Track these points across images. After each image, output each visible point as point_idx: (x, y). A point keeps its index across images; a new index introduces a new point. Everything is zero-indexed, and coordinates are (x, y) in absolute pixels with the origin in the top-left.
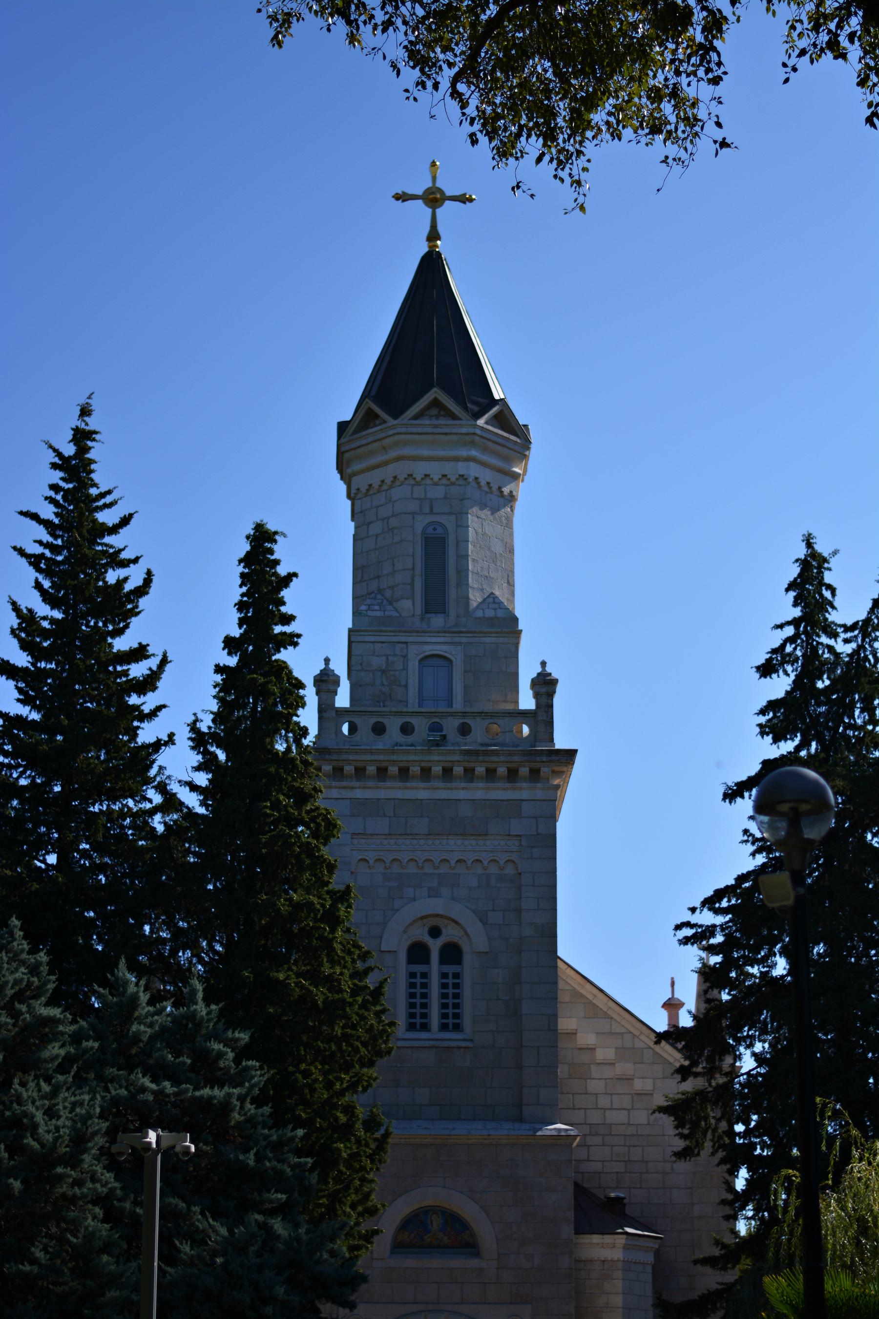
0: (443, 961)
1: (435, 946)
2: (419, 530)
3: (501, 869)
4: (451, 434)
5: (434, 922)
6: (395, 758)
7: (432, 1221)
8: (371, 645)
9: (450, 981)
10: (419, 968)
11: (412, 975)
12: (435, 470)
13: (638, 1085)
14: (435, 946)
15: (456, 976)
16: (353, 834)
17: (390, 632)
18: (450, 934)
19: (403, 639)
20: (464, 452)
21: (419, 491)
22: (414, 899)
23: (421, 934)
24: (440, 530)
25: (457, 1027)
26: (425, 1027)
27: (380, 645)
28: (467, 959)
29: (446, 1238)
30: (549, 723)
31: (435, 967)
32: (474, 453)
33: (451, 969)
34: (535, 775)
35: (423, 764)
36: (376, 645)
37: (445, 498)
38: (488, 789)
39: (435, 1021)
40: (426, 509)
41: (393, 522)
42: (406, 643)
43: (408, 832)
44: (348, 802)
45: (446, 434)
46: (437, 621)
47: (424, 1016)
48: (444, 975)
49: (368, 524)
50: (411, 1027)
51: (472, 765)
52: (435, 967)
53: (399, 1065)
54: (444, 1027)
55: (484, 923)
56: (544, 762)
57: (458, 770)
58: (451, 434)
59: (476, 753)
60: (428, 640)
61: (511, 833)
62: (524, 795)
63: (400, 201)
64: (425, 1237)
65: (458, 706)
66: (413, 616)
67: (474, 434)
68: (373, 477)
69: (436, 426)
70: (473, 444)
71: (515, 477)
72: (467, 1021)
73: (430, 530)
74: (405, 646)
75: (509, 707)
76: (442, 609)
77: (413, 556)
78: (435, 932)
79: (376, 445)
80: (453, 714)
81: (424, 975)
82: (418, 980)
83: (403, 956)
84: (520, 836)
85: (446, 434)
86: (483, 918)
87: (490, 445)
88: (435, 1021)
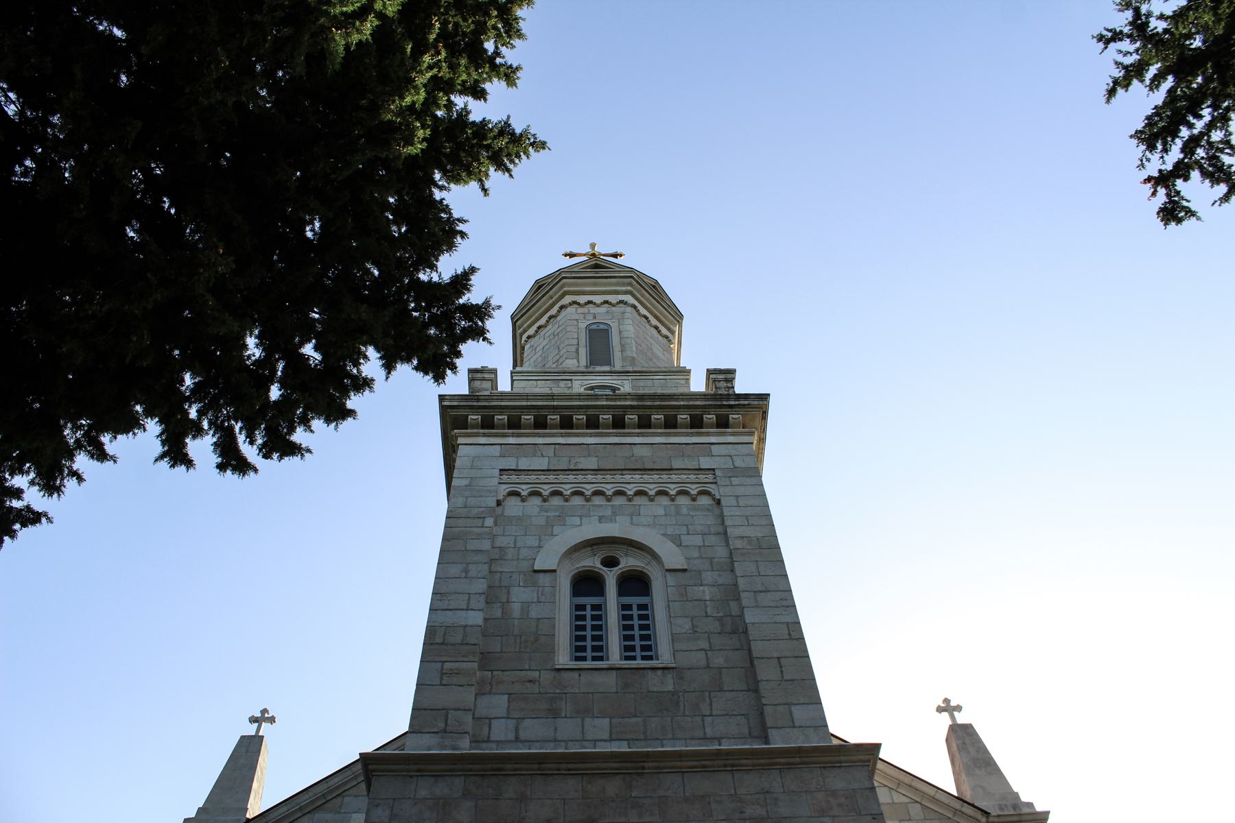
0: (621, 593)
2: (583, 325)
3: (694, 500)
4: (610, 277)
6: (555, 403)
8: (535, 382)
10: (589, 601)
12: (598, 299)
16: (501, 470)
17: (554, 373)
18: (629, 562)
19: (568, 378)
20: (624, 288)
21: (581, 310)
22: (581, 525)
23: (593, 562)
24: (602, 327)
27: (544, 382)
32: (629, 288)
34: (723, 423)
35: (590, 412)
36: (539, 382)
37: (607, 312)
38: (668, 435)
40: (590, 317)
41: (557, 331)
42: (571, 380)
43: (572, 467)
44: (499, 446)
45: (606, 277)
49: (536, 349)
51: (648, 412)
53: (558, 691)
55: (680, 545)
56: (731, 406)
57: (632, 417)
58: (610, 277)
60: (594, 378)
61: (702, 467)
62: (713, 439)
63: (568, 257)
66: (578, 367)
67: (631, 277)
69: (597, 272)
70: (630, 284)
71: (673, 333)
73: (594, 327)
74: (570, 382)
75: (681, 390)
76: (608, 362)
77: (578, 339)
78: (611, 562)
79: (544, 298)
84: (714, 470)
85: (606, 277)
86: (677, 541)
87: (647, 294)
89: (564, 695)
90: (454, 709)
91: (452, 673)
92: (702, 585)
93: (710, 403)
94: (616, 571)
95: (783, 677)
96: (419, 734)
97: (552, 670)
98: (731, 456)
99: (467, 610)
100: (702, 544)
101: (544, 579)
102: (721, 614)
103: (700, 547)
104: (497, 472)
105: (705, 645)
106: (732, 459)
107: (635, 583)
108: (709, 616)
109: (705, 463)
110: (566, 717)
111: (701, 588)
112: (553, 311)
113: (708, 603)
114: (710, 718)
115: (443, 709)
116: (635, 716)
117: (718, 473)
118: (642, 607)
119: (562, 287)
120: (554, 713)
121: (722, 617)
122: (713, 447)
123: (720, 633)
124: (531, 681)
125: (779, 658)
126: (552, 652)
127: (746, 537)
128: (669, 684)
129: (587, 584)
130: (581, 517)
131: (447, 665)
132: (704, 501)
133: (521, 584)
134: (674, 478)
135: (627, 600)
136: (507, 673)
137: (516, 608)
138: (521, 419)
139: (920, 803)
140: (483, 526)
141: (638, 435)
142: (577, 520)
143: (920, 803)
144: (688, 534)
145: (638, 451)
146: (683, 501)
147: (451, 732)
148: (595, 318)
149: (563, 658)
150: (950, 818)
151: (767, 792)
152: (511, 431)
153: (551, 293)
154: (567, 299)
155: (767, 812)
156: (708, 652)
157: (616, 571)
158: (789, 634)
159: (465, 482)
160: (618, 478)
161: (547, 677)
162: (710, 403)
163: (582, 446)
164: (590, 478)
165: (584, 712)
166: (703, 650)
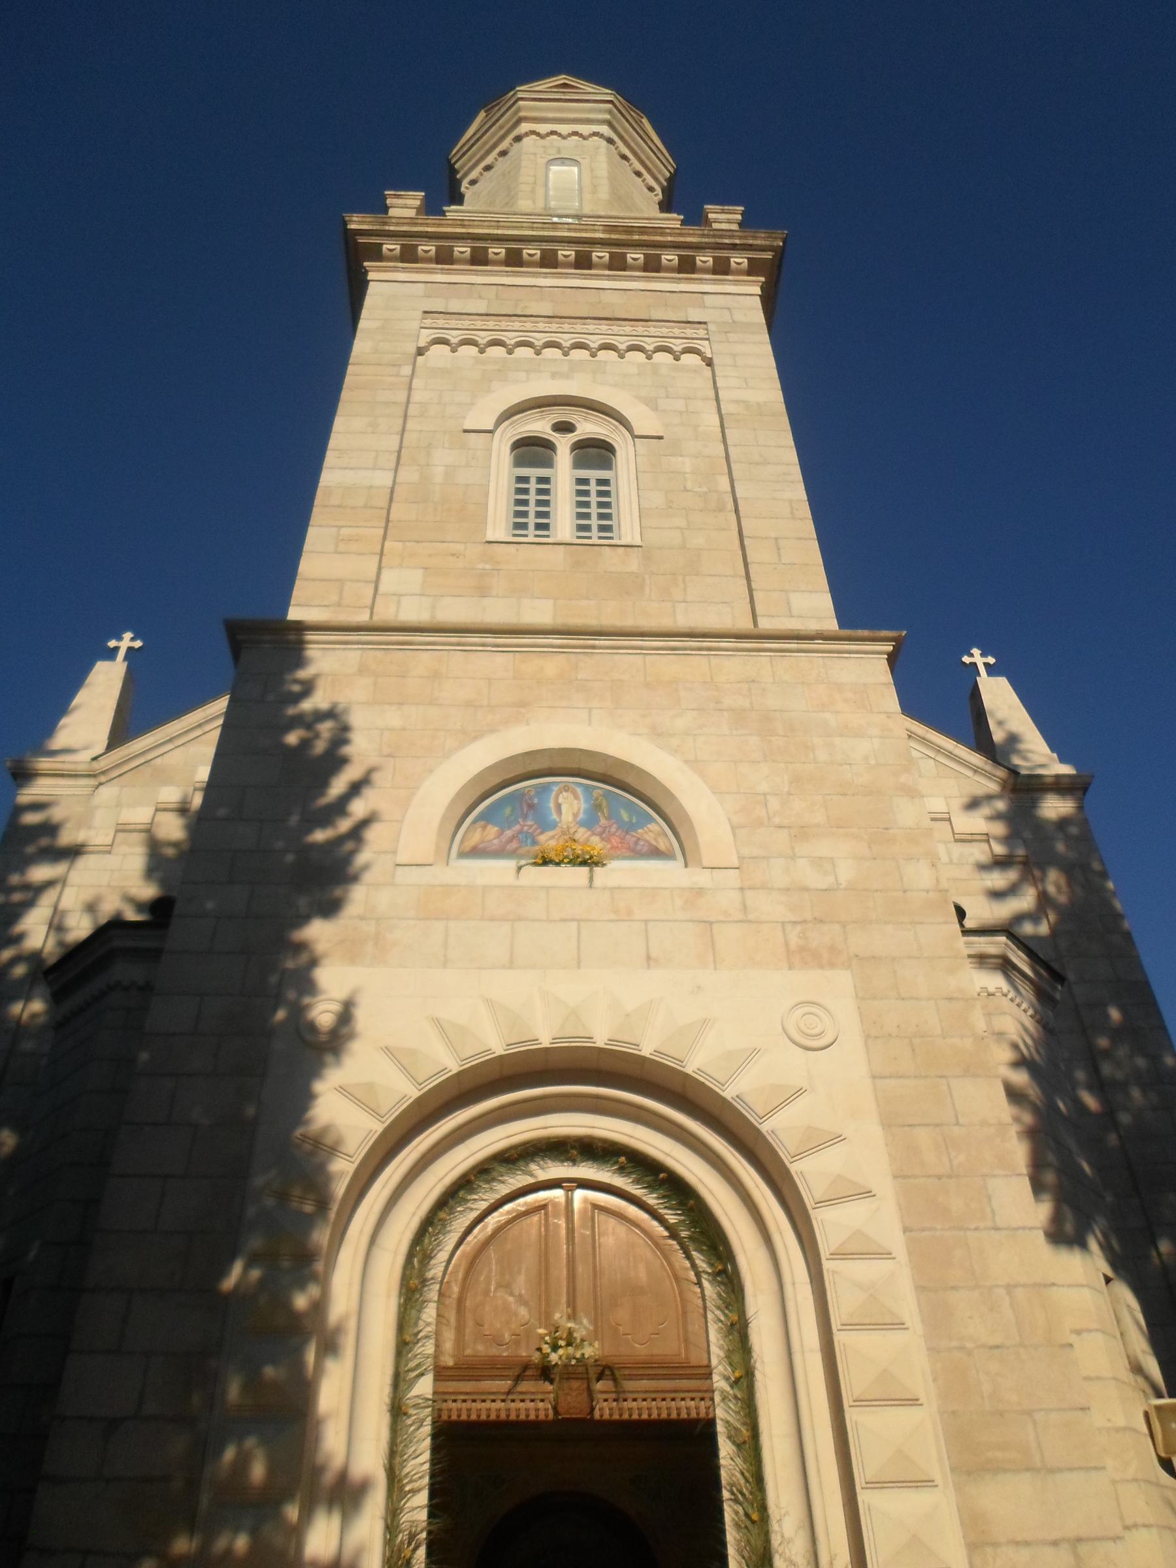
7: (559, 807)
12: (564, 129)
16: (425, 312)
18: (589, 427)
21: (541, 142)
23: (539, 425)
29: (595, 840)
35: (546, 246)
53: (488, 567)
55: (656, 409)
57: (601, 255)
64: (542, 838)
67: (610, 102)
72: (628, 529)
78: (564, 427)
79: (494, 128)
84: (705, 323)
86: (652, 403)
89: (496, 572)
90: (352, 581)
91: (349, 540)
92: (682, 456)
93: (707, 240)
94: (572, 438)
95: (780, 560)
96: (305, 608)
97: (480, 543)
98: (729, 309)
99: (374, 469)
100: (684, 409)
102: (705, 489)
103: (681, 413)
104: (419, 314)
105: (682, 523)
106: (730, 312)
108: (688, 491)
109: (694, 315)
110: (497, 596)
111: (680, 459)
113: (687, 475)
114: (683, 605)
115: (337, 580)
116: (588, 599)
117: (711, 327)
121: (706, 493)
122: (706, 297)
123: (701, 511)
124: (453, 555)
125: (776, 539)
126: (482, 521)
127: (743, 401)
128: (633, 563)
130: (527, 371)
131: (344, 531)
132: (688, 359)
133: (446, 445)
134: (653, 331)
135: (584, 473)
136: (424, 544)
137: (438, 473)
138: (453, 251)
139: (935, 759)
140: (398, 375)
141: (609, 278)
142: (523, 375)
143: (935, 759)
144: (667, 397)
145: (607, 297)
146: (662, 358)
147: (348, 606)
148: (559, 151)
149: (498, 526)
150: (969, 777)
151: (753, 681)
152: (440, 266)
153: (501, 121)
154: (524, 127)
155: (751, 703)
156: (684, 530)
157: (572, 438)
158: (792, 513)
159: (377, 324)
160: (579, 327)
162: (707, 240)
163: (534, 288)
164: (541, 326)
166: (678, 528)
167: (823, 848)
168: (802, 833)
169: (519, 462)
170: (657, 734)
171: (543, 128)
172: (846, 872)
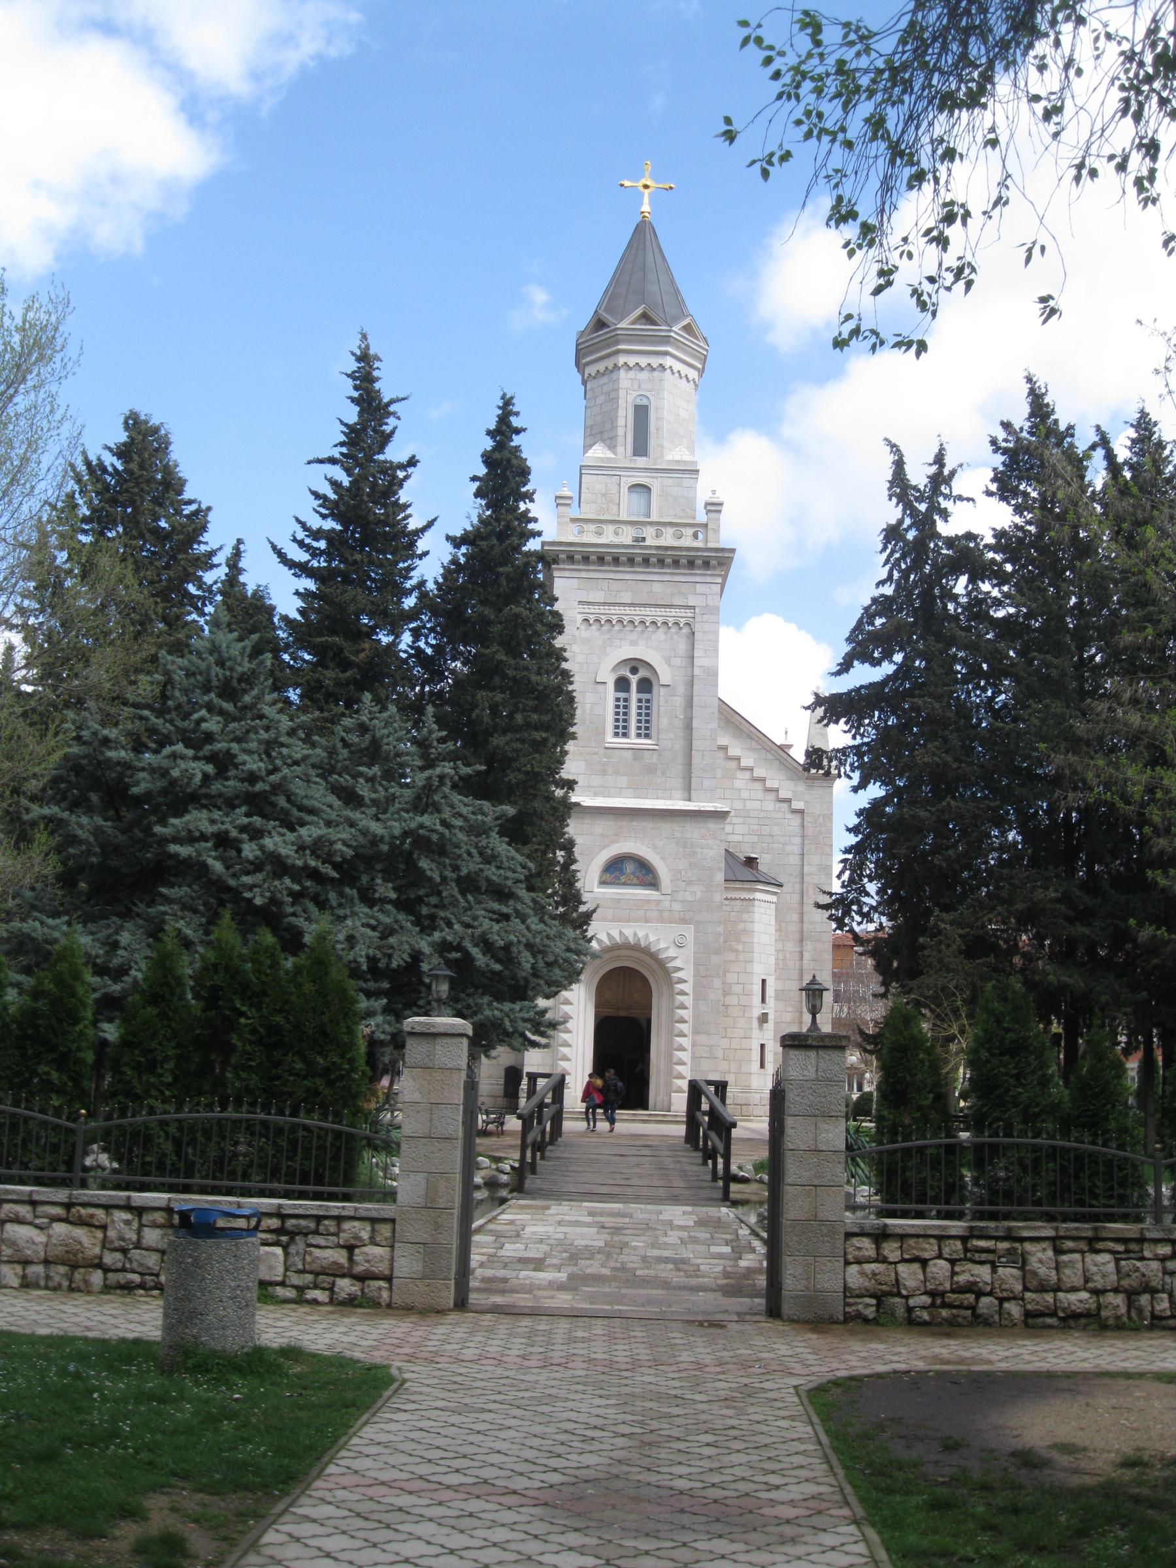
0: (639, 691)
1: (634, 680)
2: (630, 399)
5: (634, 664)
9: (644, 704)
11: (618, 700)
12: (643, 361)
13: (769, 784)
14: (634, 680)
15: (648, 701)
18: (643, 673)
21: (632, 374)
24: (645, 402)
25: (647, 736)
26: (625, 735)
28: (655, 688)
30: (717, 531)
31: (634, 695)
33: (644, 696)
39: (633, 730)
46: (641, 462)
47: (625, 727)
48: (640, 701)
50: (616, 734)
52: (634, 695)
54: (639, 735)
59: (667, 548)
65: (654, 517)
68: (601, 367)
73: (638, 402)
78: (634, 671)
80: (651, 523)
81: (626, 700)
82: (621, 703)
83: (611, 686)
86: (668, 663)
88: (633, 730)
101: (601, 687)
107: (646, 686)
112: (609, 363)
118: (648, 701)
119: (617, 342)
120: (604, 773)
129: (622, 684)
137: (588, 706)
154: (622, 360)
161: (602, 751)
165: (617, 772)
167: (693, 888)
168: (689, 883)
169: (617, 690)
170: (655, 847)
171: (632, 360)
172: (699, 896)
